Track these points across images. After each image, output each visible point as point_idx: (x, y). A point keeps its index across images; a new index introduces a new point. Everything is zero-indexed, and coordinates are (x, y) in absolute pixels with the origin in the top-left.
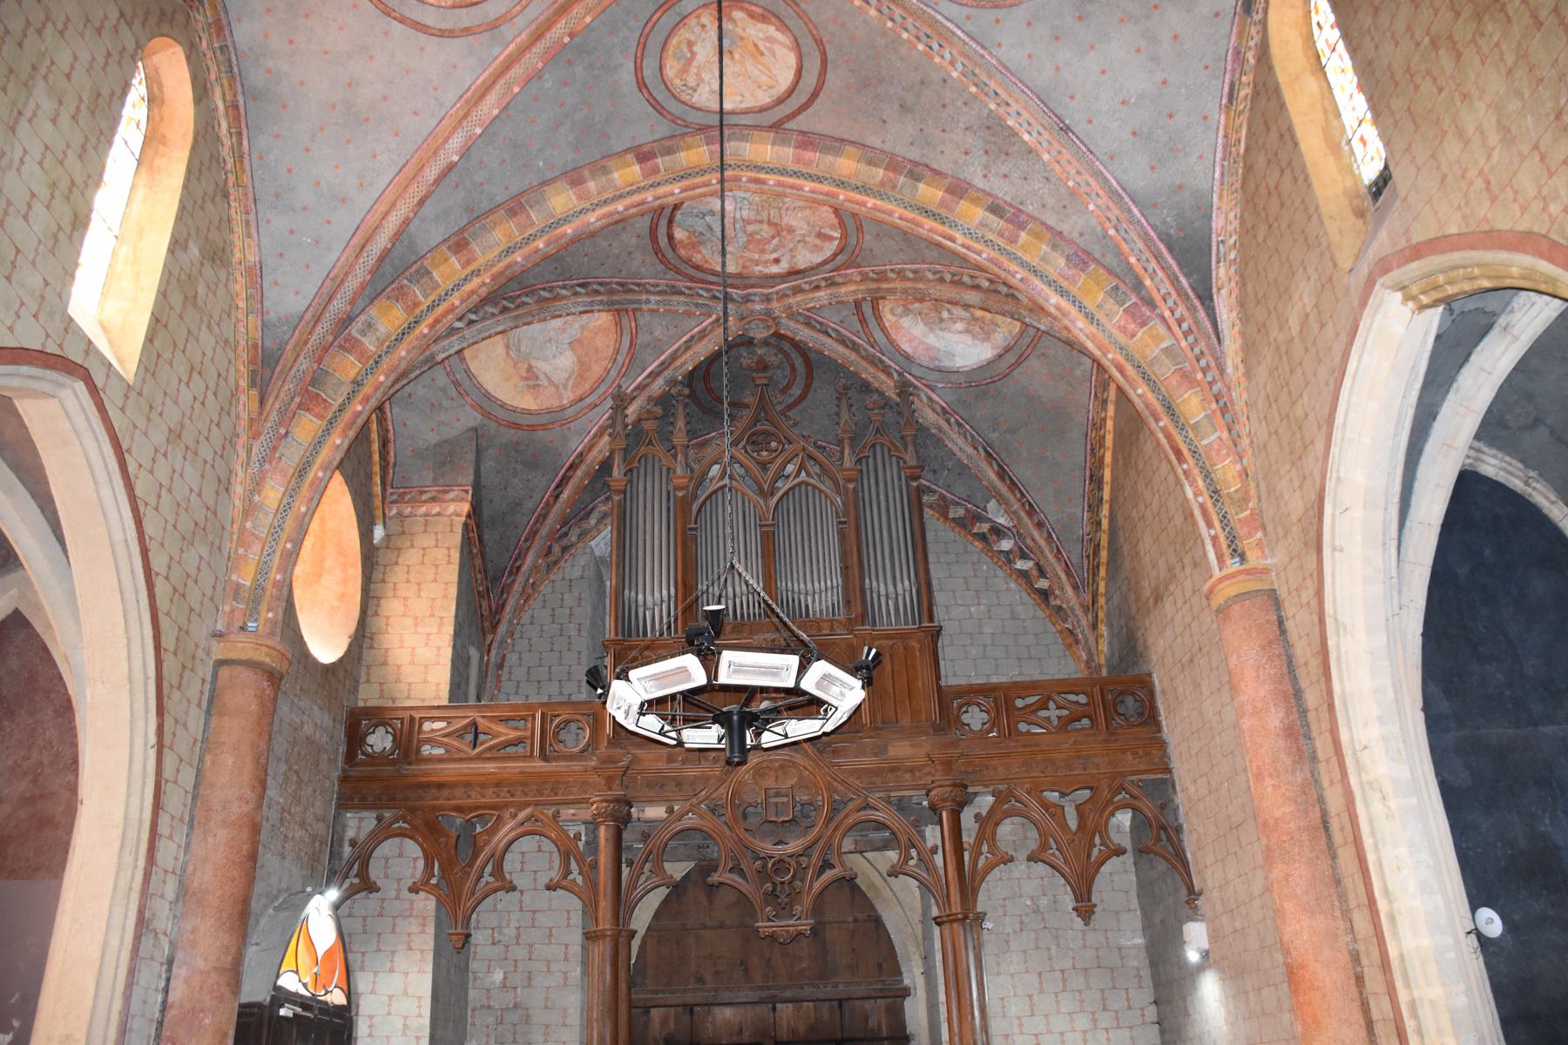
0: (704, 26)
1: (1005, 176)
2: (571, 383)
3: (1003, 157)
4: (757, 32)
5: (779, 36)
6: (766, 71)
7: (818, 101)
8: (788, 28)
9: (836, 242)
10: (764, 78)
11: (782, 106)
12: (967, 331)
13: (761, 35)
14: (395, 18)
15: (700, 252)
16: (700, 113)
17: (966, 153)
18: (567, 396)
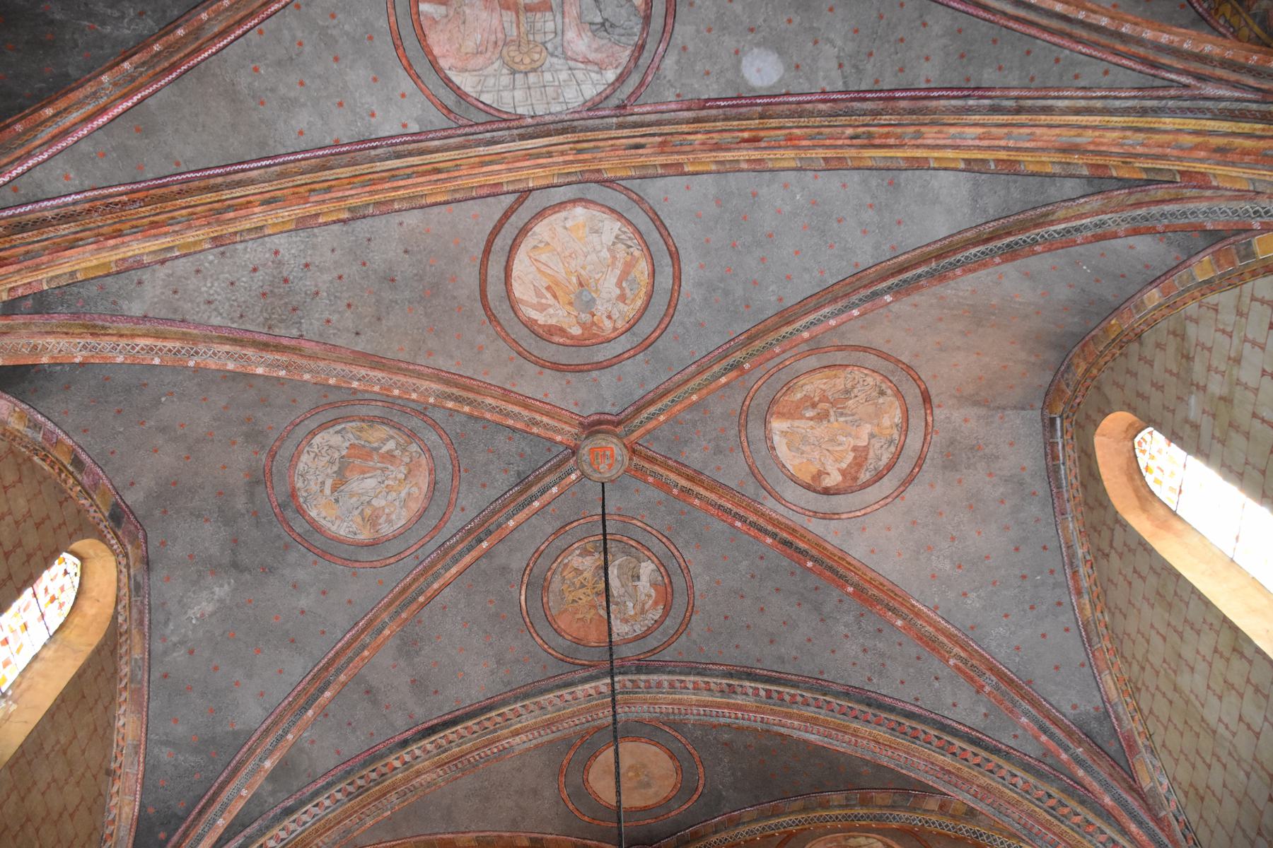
0: (609, 317)
1: (255, 270)
3: (267, 289)
4: (555, 314)
5: (534, 314)
6: (543, 268)
7: (482, 246)
8: (526, 326)
10: (544, 258)
11: (521, 224)
13: (551, 311)
16: (610, 204)
17: (307, 265)
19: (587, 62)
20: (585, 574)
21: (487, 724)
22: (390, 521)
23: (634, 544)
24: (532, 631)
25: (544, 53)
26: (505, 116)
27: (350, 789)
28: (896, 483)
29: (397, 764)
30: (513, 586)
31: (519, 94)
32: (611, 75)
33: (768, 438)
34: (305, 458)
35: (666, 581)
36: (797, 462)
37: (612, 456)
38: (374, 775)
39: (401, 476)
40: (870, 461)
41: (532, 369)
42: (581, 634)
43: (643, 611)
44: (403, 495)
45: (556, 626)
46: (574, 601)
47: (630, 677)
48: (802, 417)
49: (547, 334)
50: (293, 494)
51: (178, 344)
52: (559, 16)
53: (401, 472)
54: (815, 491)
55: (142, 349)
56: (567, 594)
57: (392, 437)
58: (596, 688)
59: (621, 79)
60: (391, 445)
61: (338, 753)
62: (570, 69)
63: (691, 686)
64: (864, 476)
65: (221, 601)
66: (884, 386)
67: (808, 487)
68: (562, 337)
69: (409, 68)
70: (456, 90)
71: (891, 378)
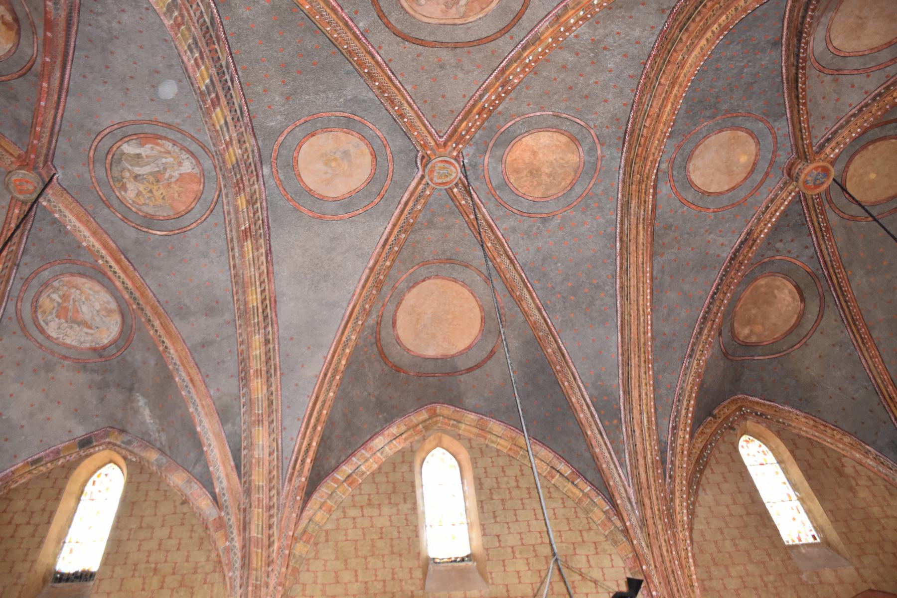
20: (141, 189)
22: (108, 302)
23: (110, 157)
24: (185, 230)
30: (150, 239)
34: (68, 341)
35: (135, 137)
37: (20, 180)
39: (78, 292)
42: (192, 195)
44: (91, 292)
45: (183, 213)
46: (163, 198)
50: (94, 350)
53: (74, 293)
56: (157, 203)
57: (49, 296)
61: (232, 376)
65: (145, 404)
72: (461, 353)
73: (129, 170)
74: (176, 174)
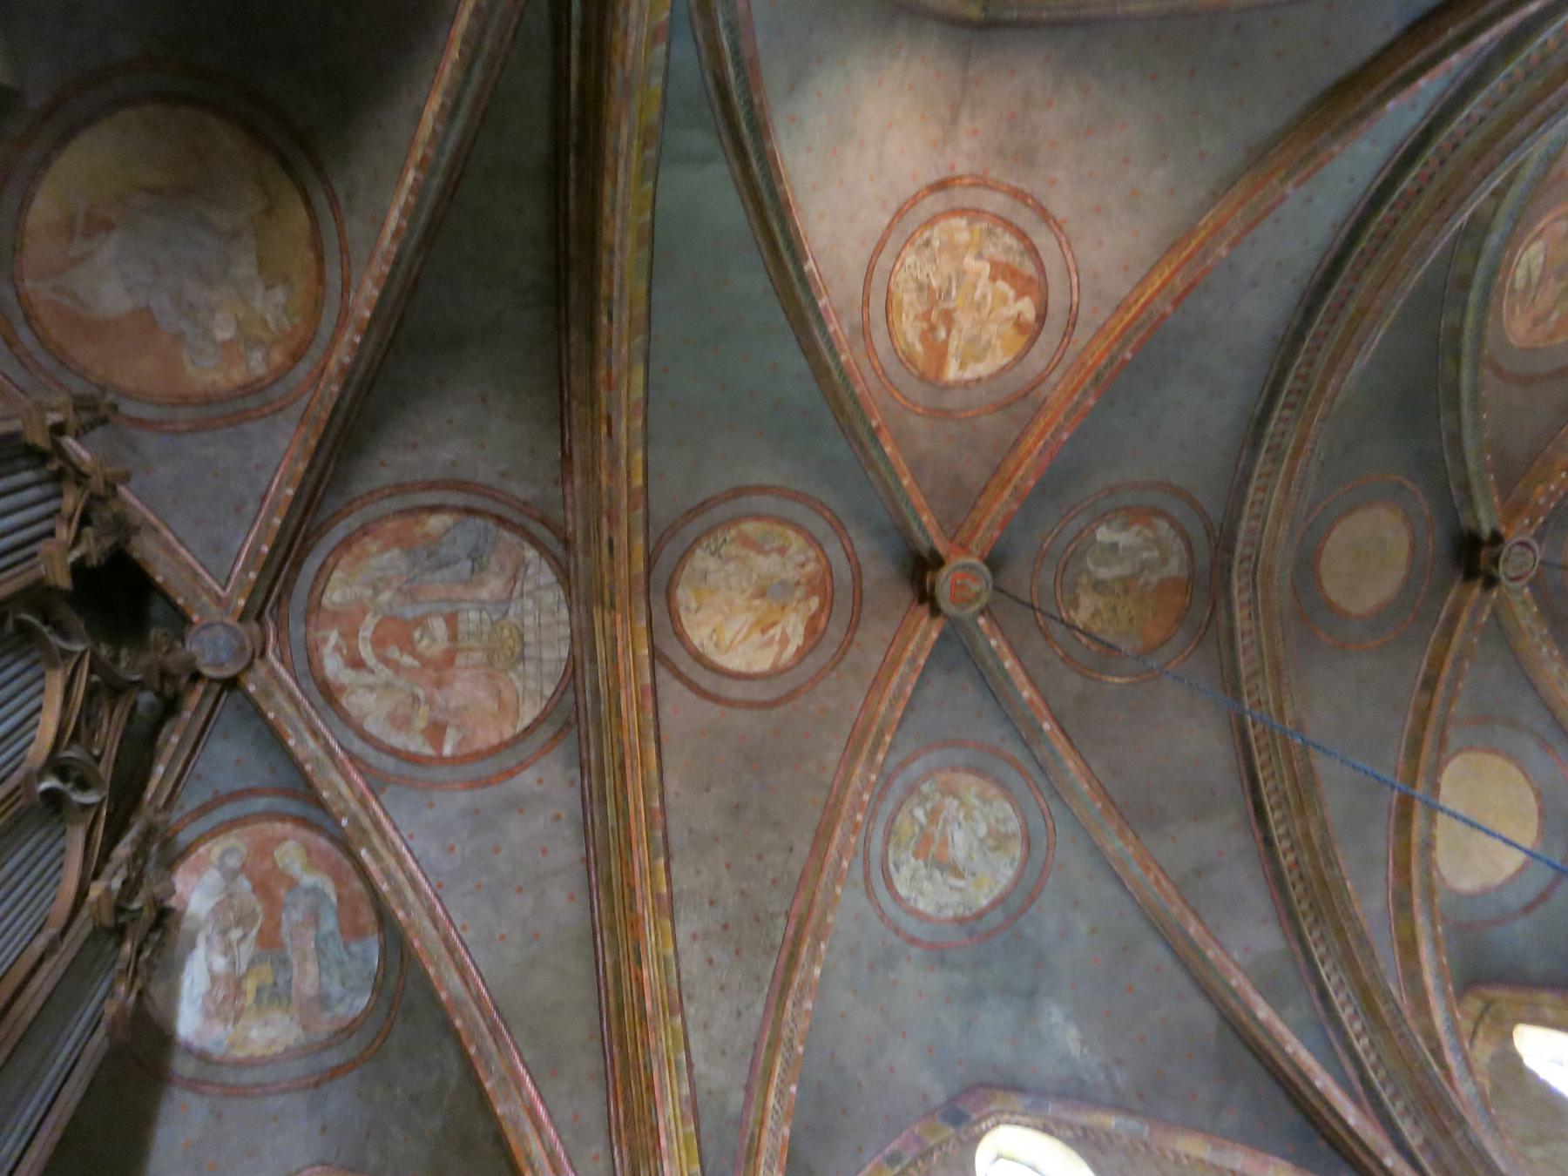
0: (803, 565)
1: (710, 961)
2: (67, 302)
4: (794, 627)
5: (791, 649)
6: (741, 636)
7: (708, 704)
9: (428, 751)
11: (690, 660)
12: (214, 979)
13: (789, 630)
14: (893, 219)
15: (386, 548)
17: (712, 903)
18: (39, 290)
19: (514, 578)
21: (1262, 742)
22: (1005, 821)
25: (503, 622)
26: (570, 671)
27: (1310, 918)
28: (1044, 228)
29: (1291, 858)
31: (547, 654)
32: (531, 554)
33: (966, 385)
36: (999, 352)
38: (1300, 887)
39: (956, 803)
40: (1011, 260)
41: (853, 655)
43: (1157, 542)
47: (1236, 564)
48: (945, 343)
49: (813, 631)
50: (960, 921)
51: (779, 1060)
52: (464, 606)
53: (951, 804)
54: (1038, 333)
55: (779, 1102)
57: (911, 812)
58: (1242, 606)
59: (535, 542)
60: (919, 813)
62: (522, 595)
63: (1260, 496)
64: (1029, 268)
66: (919, 241)
67: (1033, 341)
68: (820, 618)
69: (510, 773)
70: (538, 722)
71: (910, 233)
72: (1512, 879)
73: (1089, 573)
74: (1155, 579)
